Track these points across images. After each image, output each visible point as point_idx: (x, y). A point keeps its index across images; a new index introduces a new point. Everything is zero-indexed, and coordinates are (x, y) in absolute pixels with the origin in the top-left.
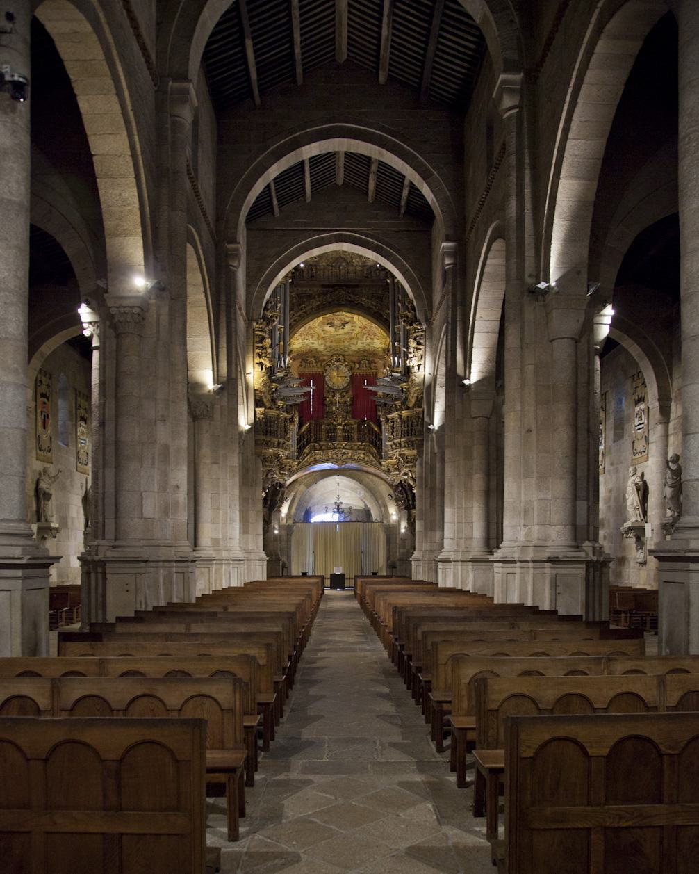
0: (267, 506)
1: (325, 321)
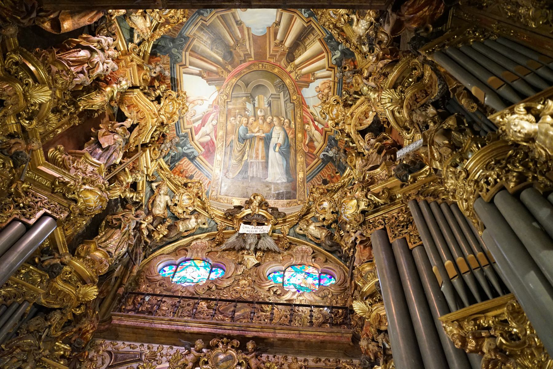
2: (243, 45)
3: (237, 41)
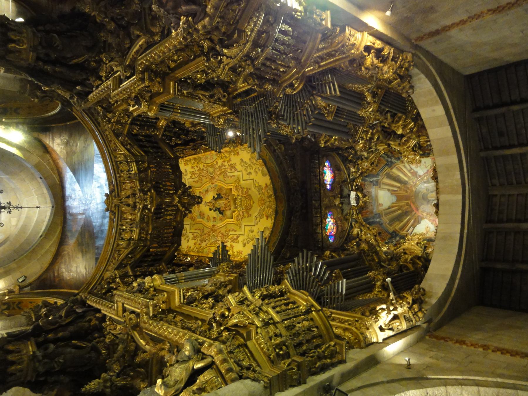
0: (41, 63)
1: (224, 191)
2: (402, 206)
3: (399, 209)
